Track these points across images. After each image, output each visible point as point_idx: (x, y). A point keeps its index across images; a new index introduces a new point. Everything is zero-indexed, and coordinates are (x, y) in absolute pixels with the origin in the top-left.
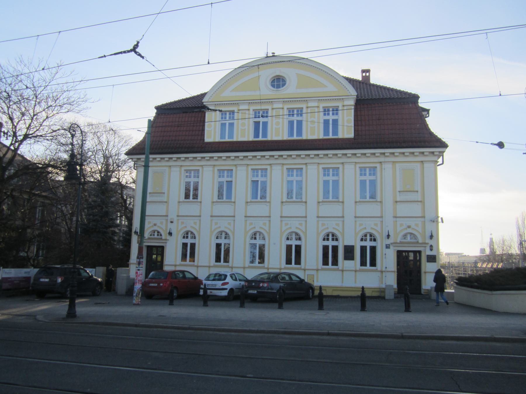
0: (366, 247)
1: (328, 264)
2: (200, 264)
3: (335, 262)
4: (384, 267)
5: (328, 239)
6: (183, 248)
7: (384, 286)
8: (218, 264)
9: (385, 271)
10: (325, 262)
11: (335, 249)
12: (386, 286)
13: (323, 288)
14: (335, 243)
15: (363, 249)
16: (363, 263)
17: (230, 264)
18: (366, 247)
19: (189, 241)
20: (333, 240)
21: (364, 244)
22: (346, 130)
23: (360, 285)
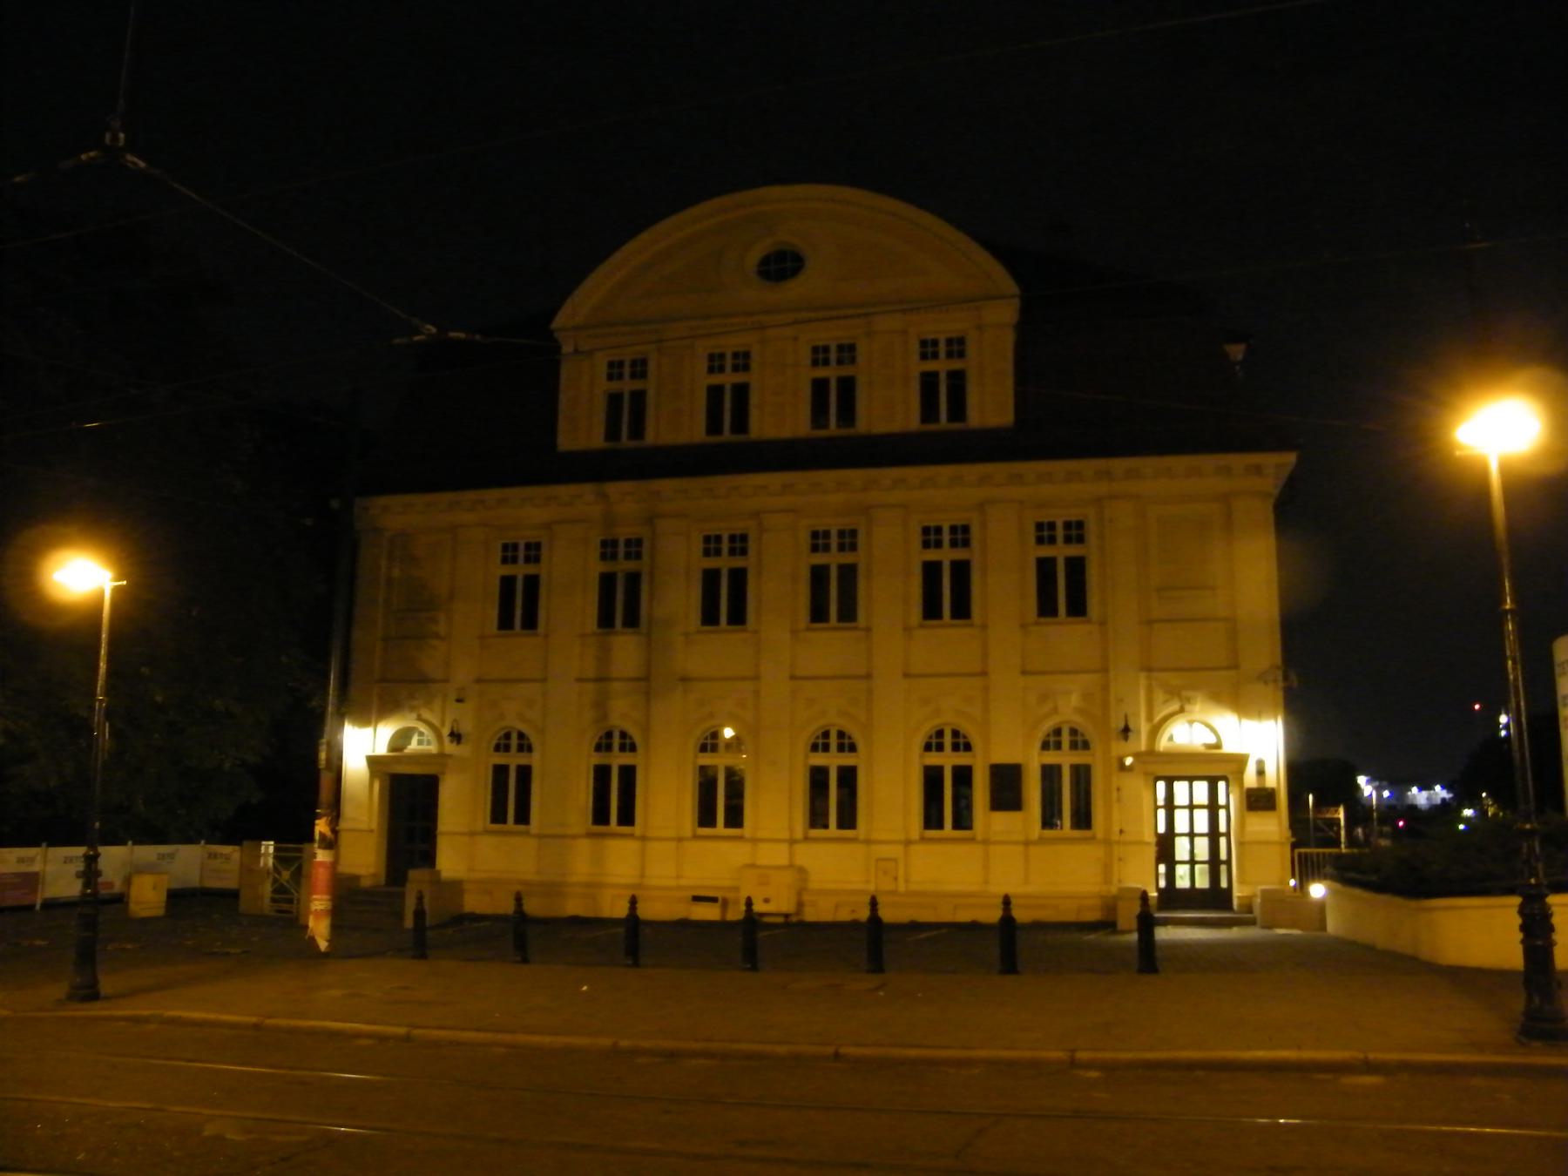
0: (1059, 768)
1: (940, 826)
2: (761, 834)
3: (963, 820)
4: (1116, 829)
5: (940, 748)
6: (596, 779)
7: (1114, 890)
8: (1049, 833)
9: (1118, 843)
10: (932, 819)
11: (963, 776)
12: (1122, 890)
13: (1013, 901)
14: (962, 759)
15: (1050, 774)
16: (1050, 819)
17: (747, 830)
18: (1059, 768)
19: (513, 760)
20: (956, 747)
21: (1051, 758)
22: (991, 404)
23: (1000, 887)
